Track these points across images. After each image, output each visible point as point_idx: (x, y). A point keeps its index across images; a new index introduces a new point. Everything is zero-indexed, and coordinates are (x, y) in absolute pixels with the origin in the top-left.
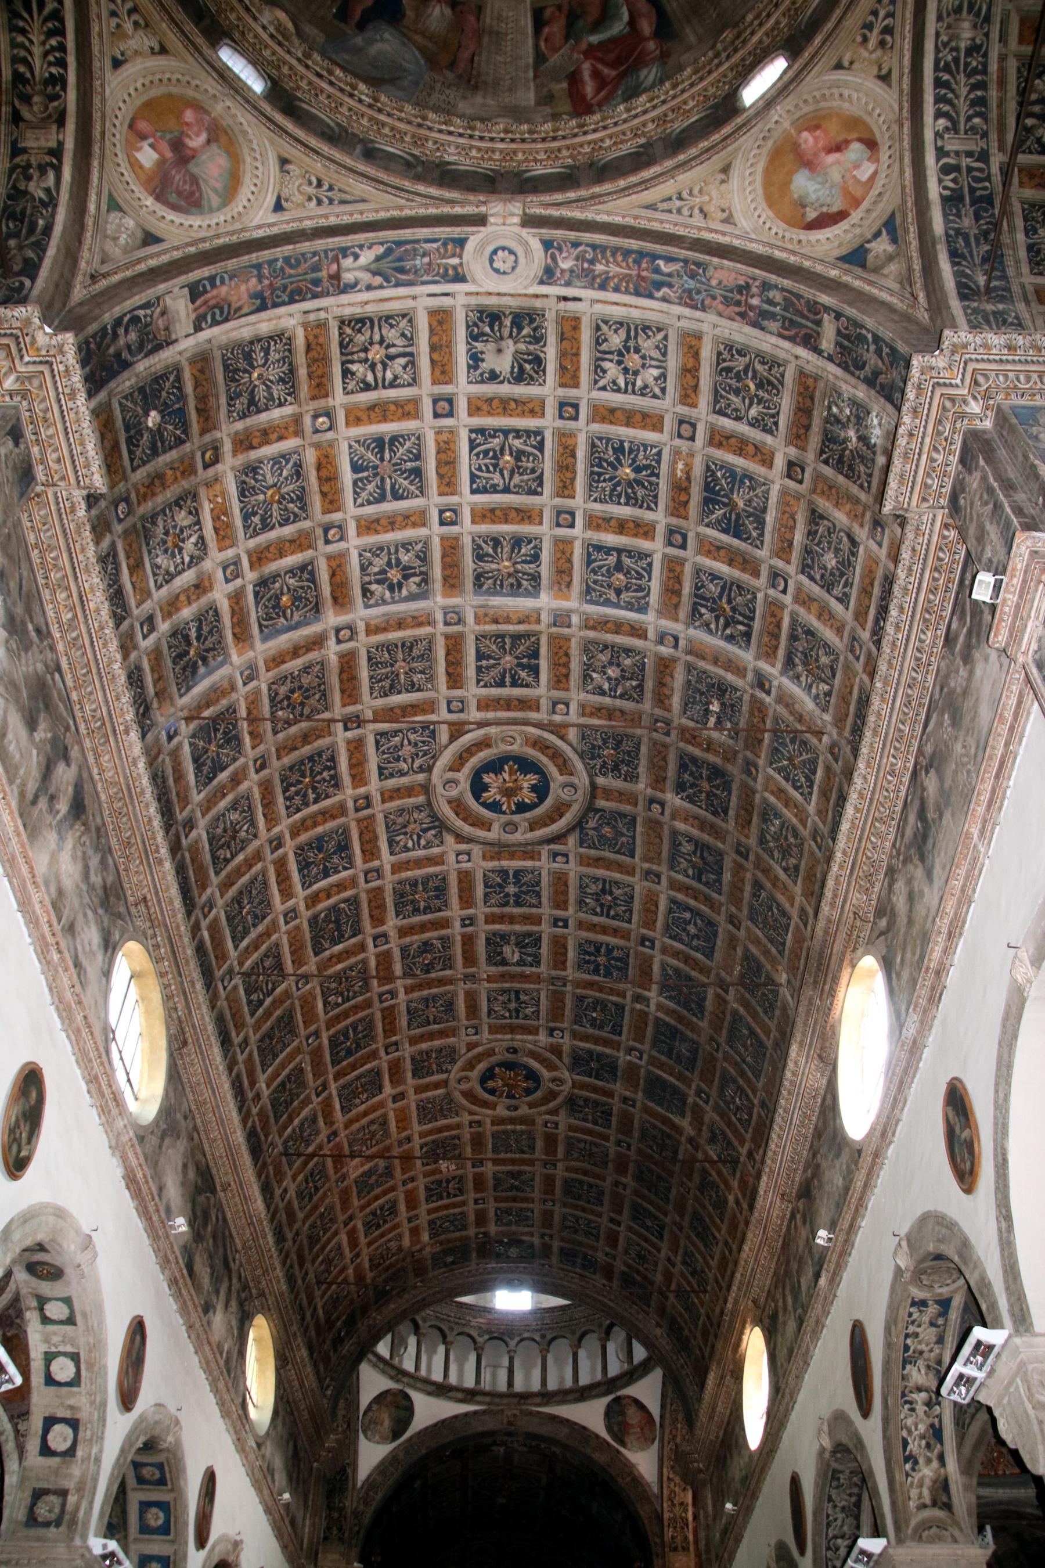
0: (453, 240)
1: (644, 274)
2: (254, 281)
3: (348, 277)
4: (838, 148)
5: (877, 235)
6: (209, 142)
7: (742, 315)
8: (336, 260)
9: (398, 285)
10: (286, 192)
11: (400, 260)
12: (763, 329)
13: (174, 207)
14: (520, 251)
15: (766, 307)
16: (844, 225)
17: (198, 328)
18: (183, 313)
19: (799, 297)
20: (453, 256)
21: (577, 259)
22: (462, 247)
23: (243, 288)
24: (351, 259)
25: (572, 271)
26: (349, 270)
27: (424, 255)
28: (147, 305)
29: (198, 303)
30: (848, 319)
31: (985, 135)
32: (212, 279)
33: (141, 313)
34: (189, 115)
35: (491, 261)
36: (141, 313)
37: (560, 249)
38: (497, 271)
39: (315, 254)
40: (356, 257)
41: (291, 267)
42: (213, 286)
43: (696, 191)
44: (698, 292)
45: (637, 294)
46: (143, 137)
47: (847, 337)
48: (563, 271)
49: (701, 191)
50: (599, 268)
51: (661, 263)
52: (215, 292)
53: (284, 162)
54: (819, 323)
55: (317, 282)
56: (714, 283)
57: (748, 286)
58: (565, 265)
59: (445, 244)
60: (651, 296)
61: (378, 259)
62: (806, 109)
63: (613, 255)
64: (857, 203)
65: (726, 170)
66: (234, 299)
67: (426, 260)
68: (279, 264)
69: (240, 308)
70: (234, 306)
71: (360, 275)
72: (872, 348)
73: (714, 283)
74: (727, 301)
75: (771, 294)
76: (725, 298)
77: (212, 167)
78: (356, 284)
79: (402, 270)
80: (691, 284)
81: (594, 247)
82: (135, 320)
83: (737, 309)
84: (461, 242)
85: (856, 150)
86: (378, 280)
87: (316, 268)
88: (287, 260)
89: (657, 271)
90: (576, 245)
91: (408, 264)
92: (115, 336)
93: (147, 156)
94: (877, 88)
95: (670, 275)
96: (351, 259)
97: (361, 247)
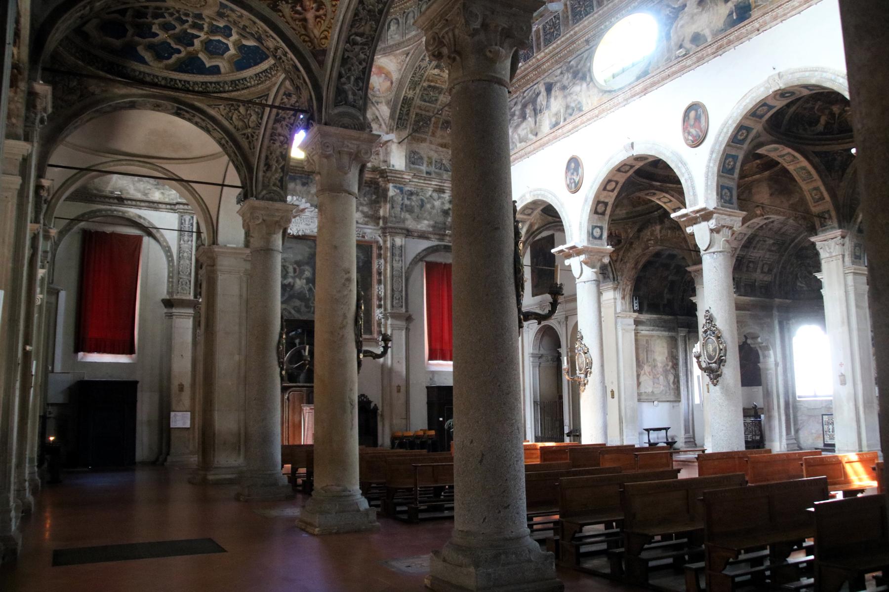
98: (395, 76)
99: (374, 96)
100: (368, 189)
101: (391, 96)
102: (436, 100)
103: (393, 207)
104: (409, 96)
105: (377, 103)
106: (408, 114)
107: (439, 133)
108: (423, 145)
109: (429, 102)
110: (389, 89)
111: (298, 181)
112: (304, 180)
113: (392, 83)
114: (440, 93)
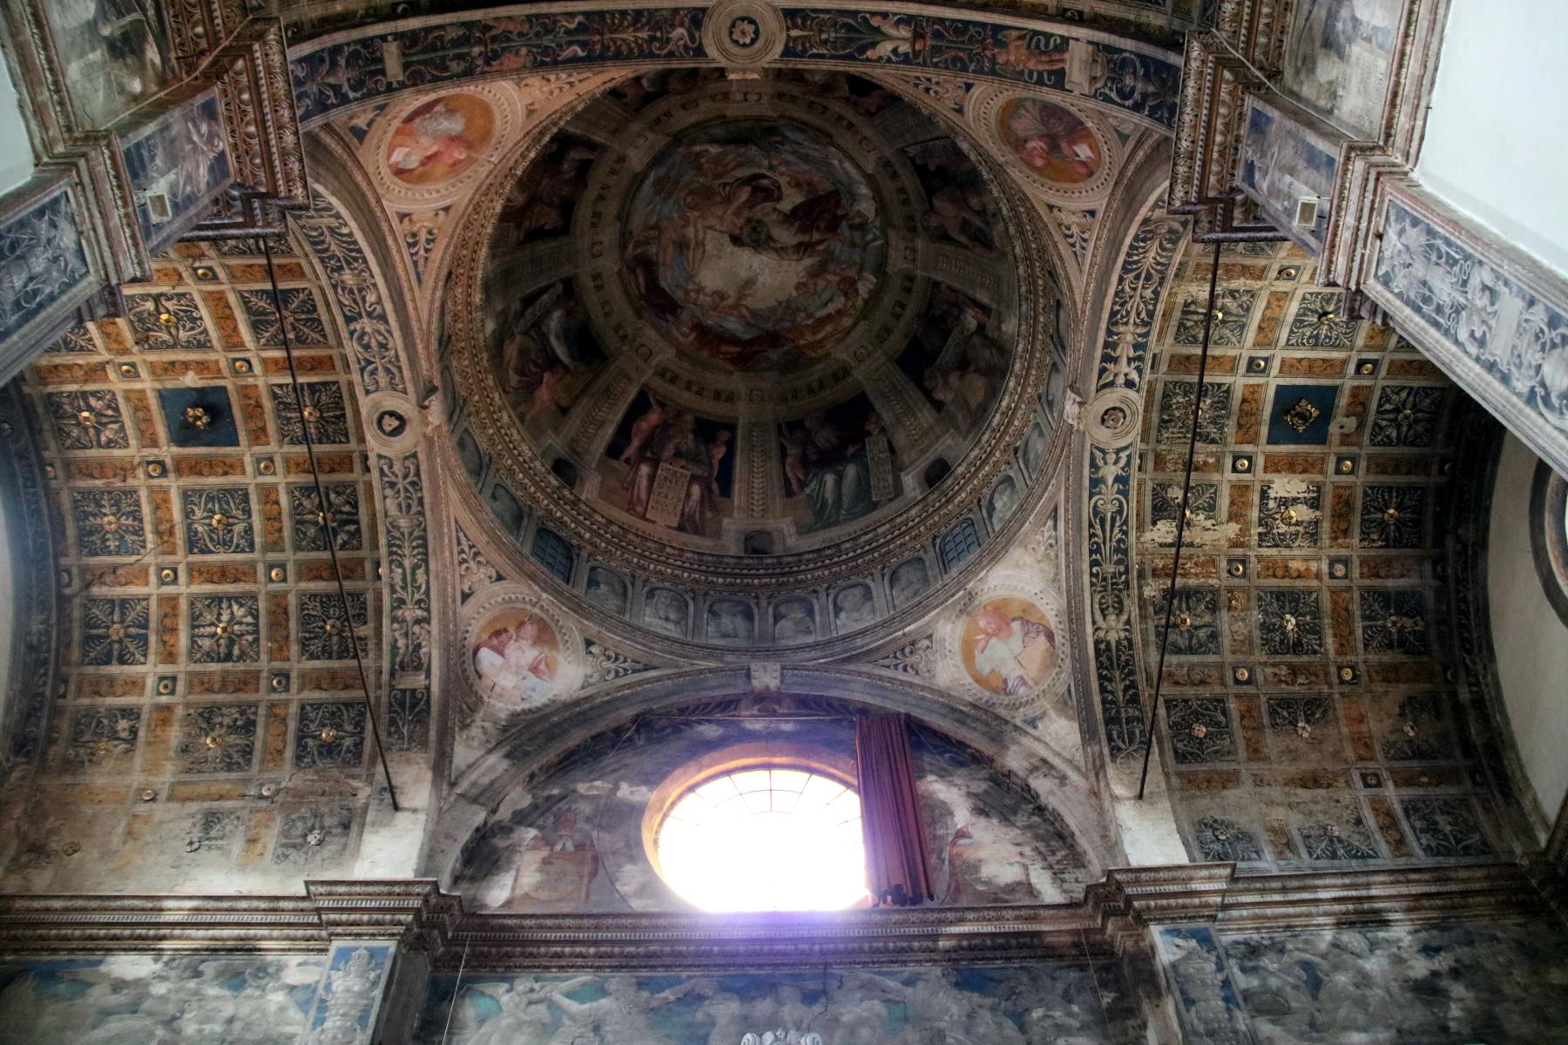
0: (796, 55)
1: (597, 38)
2: (1001, 59)
3: (904, 32)
4: (429, 158)
5: (369, 125)
6: (1026, 141)
7: (487, 28)
8: (916, 54)
9: (857, 12)
10: (961, 92)
11: (850, 40)
12: (463, 24)
13: (1069, 113)
14: (728, 44)
15: (465, 50)
16: (404, 115)
17: (1065, 40)
18: (1076, 66)
19: (435, 79)
20: (796, 39)
21: (668, 40)
22: (786, 46)
23: (1012, 58)
24: (901, 50)
25: (673, 26)
26: (904, 39)
27: (826, 42)
28: (1108, 99)
29: (1060, 66)
30: (379, 93)
31: (303, 227)
32: (1040, 82)
33: (1113, 95)
34: (1039, 162)
35: (757, 32)
36: (1113, 95)
37: (686, 47)
38: (752, 21)
39: (936, 65)
40: (895, 51)
41: (961, 60)
42: (1040, 74)
43: (556, 92)
44: (537, 34)
45: (601, 14)
46: (1083, 163)
47: (373, 74)
48: (682, 25)
49: (551, 93)
50: (644, 35)
51: (581, 53)
52: (1041, 67)
53: (960, 110)
54: (406, 66)
55: (937, 35)
56: (524, 51)
57: (488, 63)
58: (680, 31)
59: (804, 51)
60: (586, 14)
61: (874, 45)
62: (467, 173)
63: (631, 50)
64: (398, 132)
65: (530, 113)
66: (1023, 51)
67: (824, 36)
68: (972, 67)
69: (1021, 38)
70: (1024, 43)
71: (893, 32)
72: (346, 88)
73: (524, 51)
74: (506, 36)
75: (463, 66)
76: (509, 40)
77: (1025, 124)
78: (898, 23)
79: (849, 28)
80: (547, 41)
81: (651, 55)
82: (1120, 92)
83: (493, 33)
84: (788, 52)
85: (413, 163)
86: (875, 22)
87: (937, 50)
88: (965, 69)
89: (583, 45)
90: (671, 55)
91: (842, 33)
92: (1145, 96)
93: (1083, 151)
94: (404, 208)
95: (570, 44)
96: (901, 50)
97: (889, 60)
98: (1051, 608)
99: (1015, 707)
100: (1074, 975)
101: (1064, 679)
102: (1214, 636)
103: (1189, 1002)
104: (1113, 637)
105: (1032, 723)
106: (1134, 700)
107: (1272, 743)
108: (1232, 795)
109: (1191, 650)
110: (1051, 659)
111: (786, 992)
112: (812, 985)
113: (1050, 636)
114: (1213, 608)
